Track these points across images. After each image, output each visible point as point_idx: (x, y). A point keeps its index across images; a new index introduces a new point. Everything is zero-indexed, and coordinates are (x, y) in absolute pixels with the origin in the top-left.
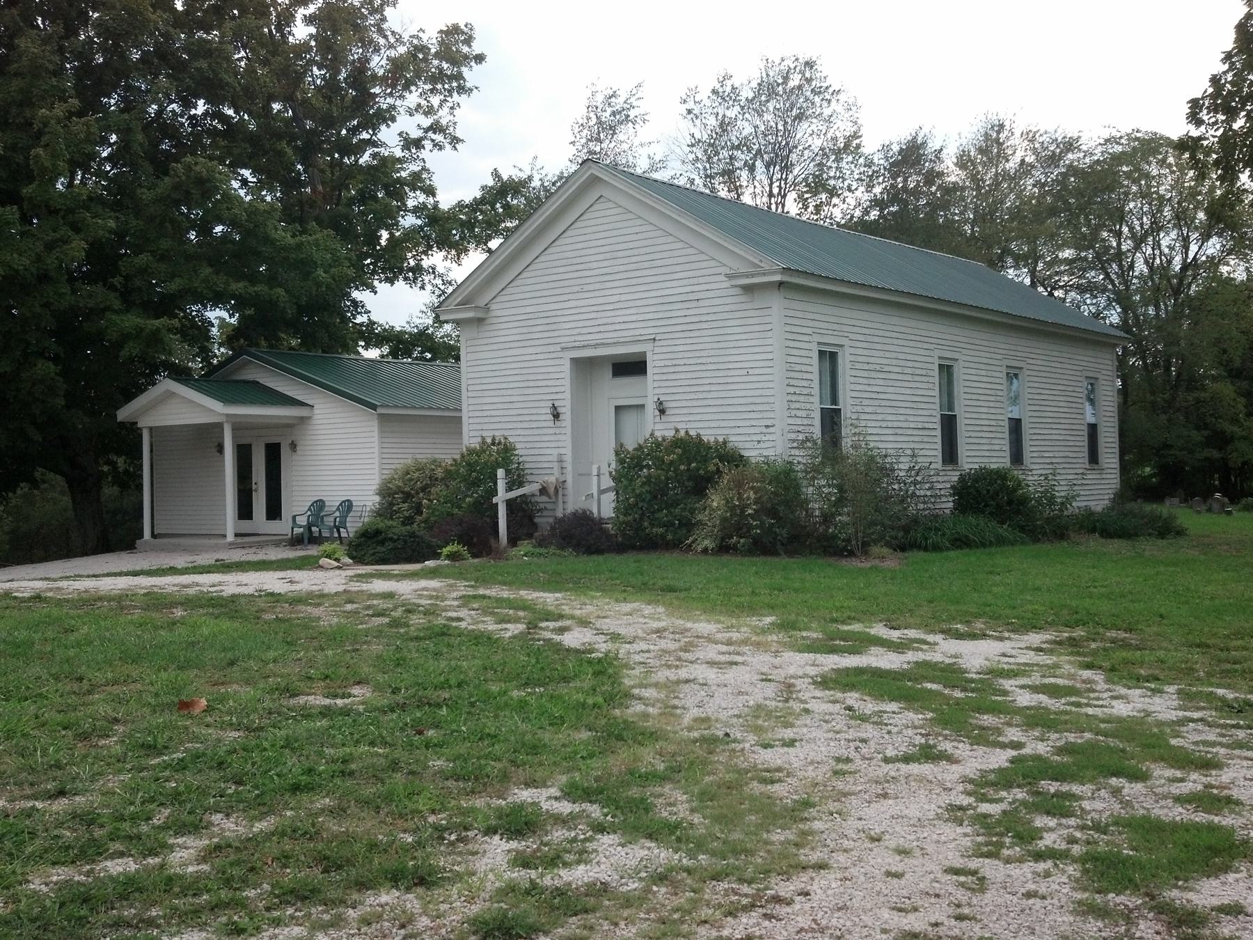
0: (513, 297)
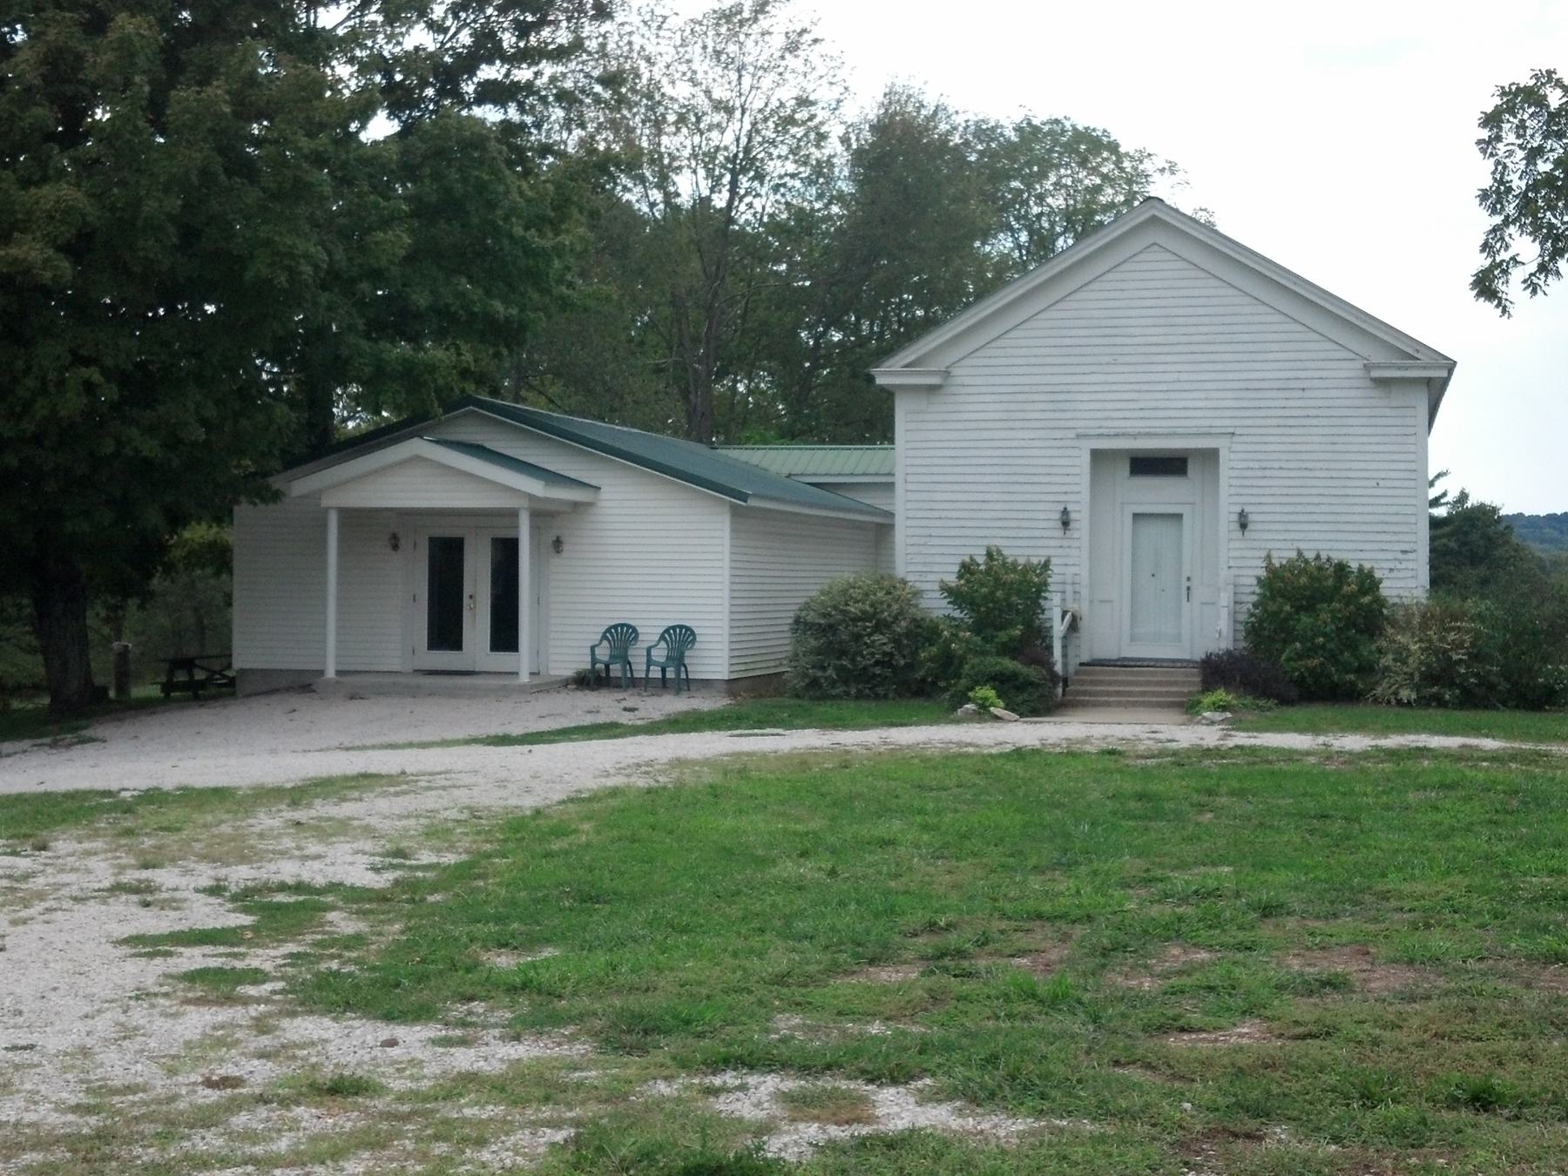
0: (993, 361)
